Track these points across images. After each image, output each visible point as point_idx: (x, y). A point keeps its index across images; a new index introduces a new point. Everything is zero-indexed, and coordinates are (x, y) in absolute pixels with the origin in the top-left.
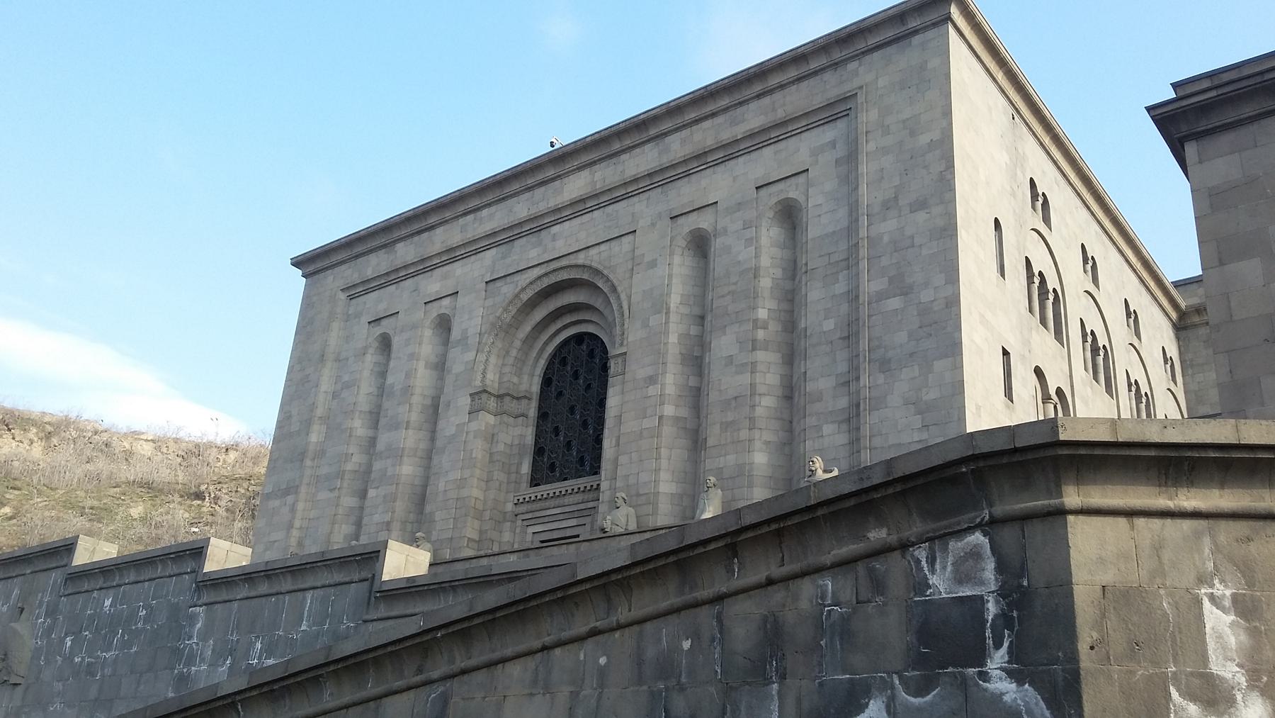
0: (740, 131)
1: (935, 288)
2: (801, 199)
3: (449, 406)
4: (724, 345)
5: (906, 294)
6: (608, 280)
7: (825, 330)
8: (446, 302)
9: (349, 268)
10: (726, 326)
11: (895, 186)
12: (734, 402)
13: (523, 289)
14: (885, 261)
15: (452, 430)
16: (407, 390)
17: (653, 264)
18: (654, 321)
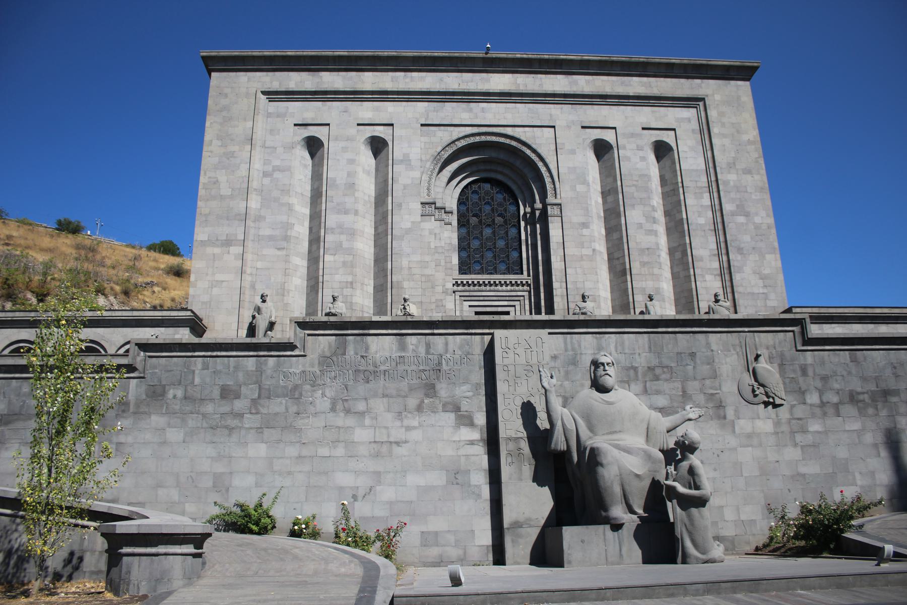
0: (631, 92)
1: (762, 217)
2: (673, 145)
3: (401, 206)
4: (634, 216)
5: (746, 216)
6: (534, 151)
7: (699, 223)
8: (381, 128)
9: (267, 76)
10: (634, 205)
11: (733, 157)
12: (647, 252)
13: (458, 139)
14: (733, 195)
15: (408, 225)
16: (351, 187)
17: (573, 152)
18: (580, 188)
